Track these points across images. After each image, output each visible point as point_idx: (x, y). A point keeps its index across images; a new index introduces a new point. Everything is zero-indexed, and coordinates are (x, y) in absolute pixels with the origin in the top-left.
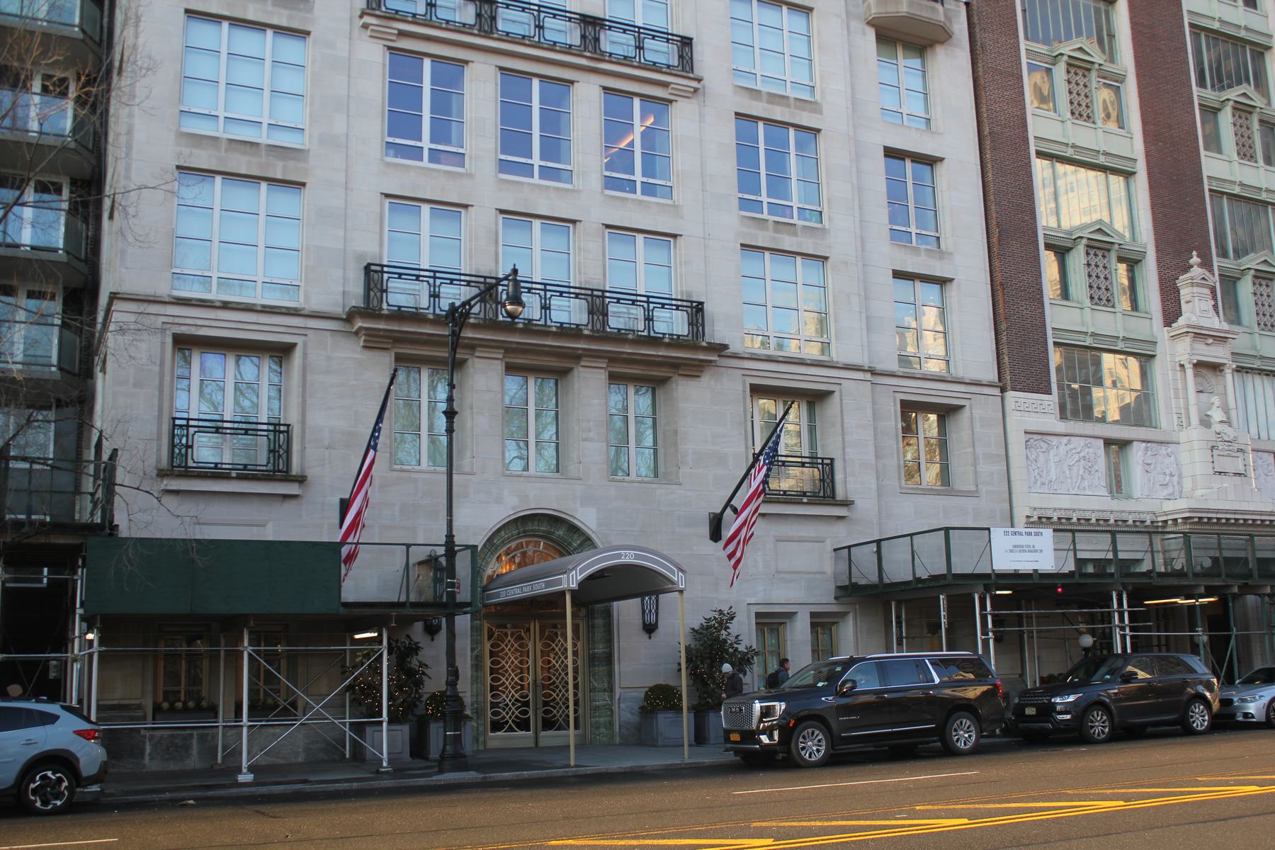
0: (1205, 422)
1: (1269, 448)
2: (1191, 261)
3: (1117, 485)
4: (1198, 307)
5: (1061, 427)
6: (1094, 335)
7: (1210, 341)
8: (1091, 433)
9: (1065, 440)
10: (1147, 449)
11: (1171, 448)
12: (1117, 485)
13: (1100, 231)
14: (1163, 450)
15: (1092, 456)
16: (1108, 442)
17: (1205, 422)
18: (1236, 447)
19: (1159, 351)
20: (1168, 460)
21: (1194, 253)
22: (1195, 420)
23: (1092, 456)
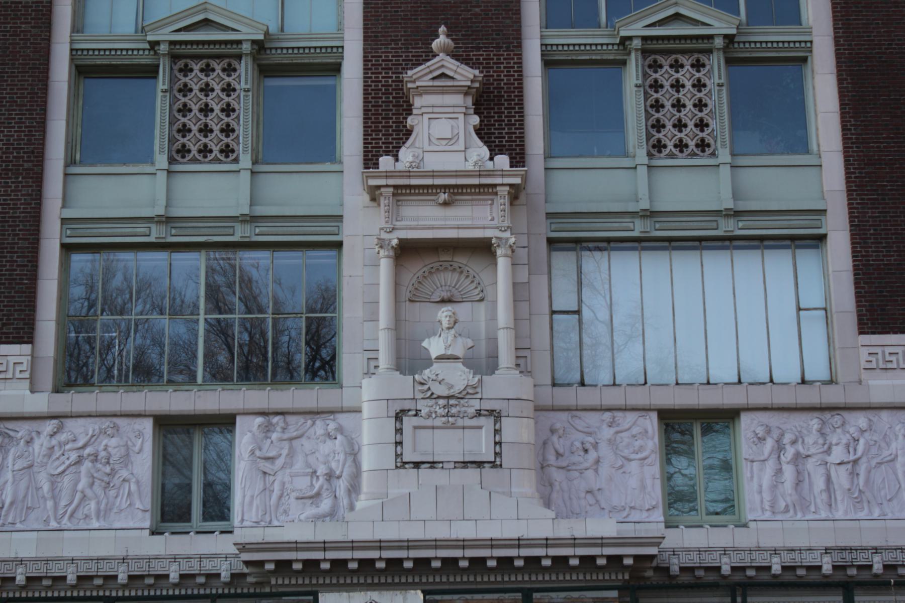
0: (409, 360)
1: (639, 397)
2: (435, 45)
3: (187, 498)
4: (443, 136)
5: (40, 402)
6: (167, 220)
7: (443, 197)
8: (116, 408)
9: (49, 426)
10: (268, 429)
11: (343, 419)
12: (187, 498)
13: (206, 23)
14: (319, 427)
15: (116, 454)
16: (166, 424)
17: (409, 360)
18: (476, 404)
19: (349, 233)
20: (326, 447)
21: (442, 29)
22: (384, 359)
23: (116, 454)
